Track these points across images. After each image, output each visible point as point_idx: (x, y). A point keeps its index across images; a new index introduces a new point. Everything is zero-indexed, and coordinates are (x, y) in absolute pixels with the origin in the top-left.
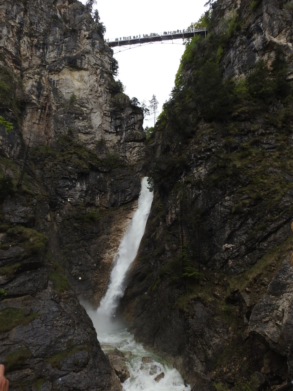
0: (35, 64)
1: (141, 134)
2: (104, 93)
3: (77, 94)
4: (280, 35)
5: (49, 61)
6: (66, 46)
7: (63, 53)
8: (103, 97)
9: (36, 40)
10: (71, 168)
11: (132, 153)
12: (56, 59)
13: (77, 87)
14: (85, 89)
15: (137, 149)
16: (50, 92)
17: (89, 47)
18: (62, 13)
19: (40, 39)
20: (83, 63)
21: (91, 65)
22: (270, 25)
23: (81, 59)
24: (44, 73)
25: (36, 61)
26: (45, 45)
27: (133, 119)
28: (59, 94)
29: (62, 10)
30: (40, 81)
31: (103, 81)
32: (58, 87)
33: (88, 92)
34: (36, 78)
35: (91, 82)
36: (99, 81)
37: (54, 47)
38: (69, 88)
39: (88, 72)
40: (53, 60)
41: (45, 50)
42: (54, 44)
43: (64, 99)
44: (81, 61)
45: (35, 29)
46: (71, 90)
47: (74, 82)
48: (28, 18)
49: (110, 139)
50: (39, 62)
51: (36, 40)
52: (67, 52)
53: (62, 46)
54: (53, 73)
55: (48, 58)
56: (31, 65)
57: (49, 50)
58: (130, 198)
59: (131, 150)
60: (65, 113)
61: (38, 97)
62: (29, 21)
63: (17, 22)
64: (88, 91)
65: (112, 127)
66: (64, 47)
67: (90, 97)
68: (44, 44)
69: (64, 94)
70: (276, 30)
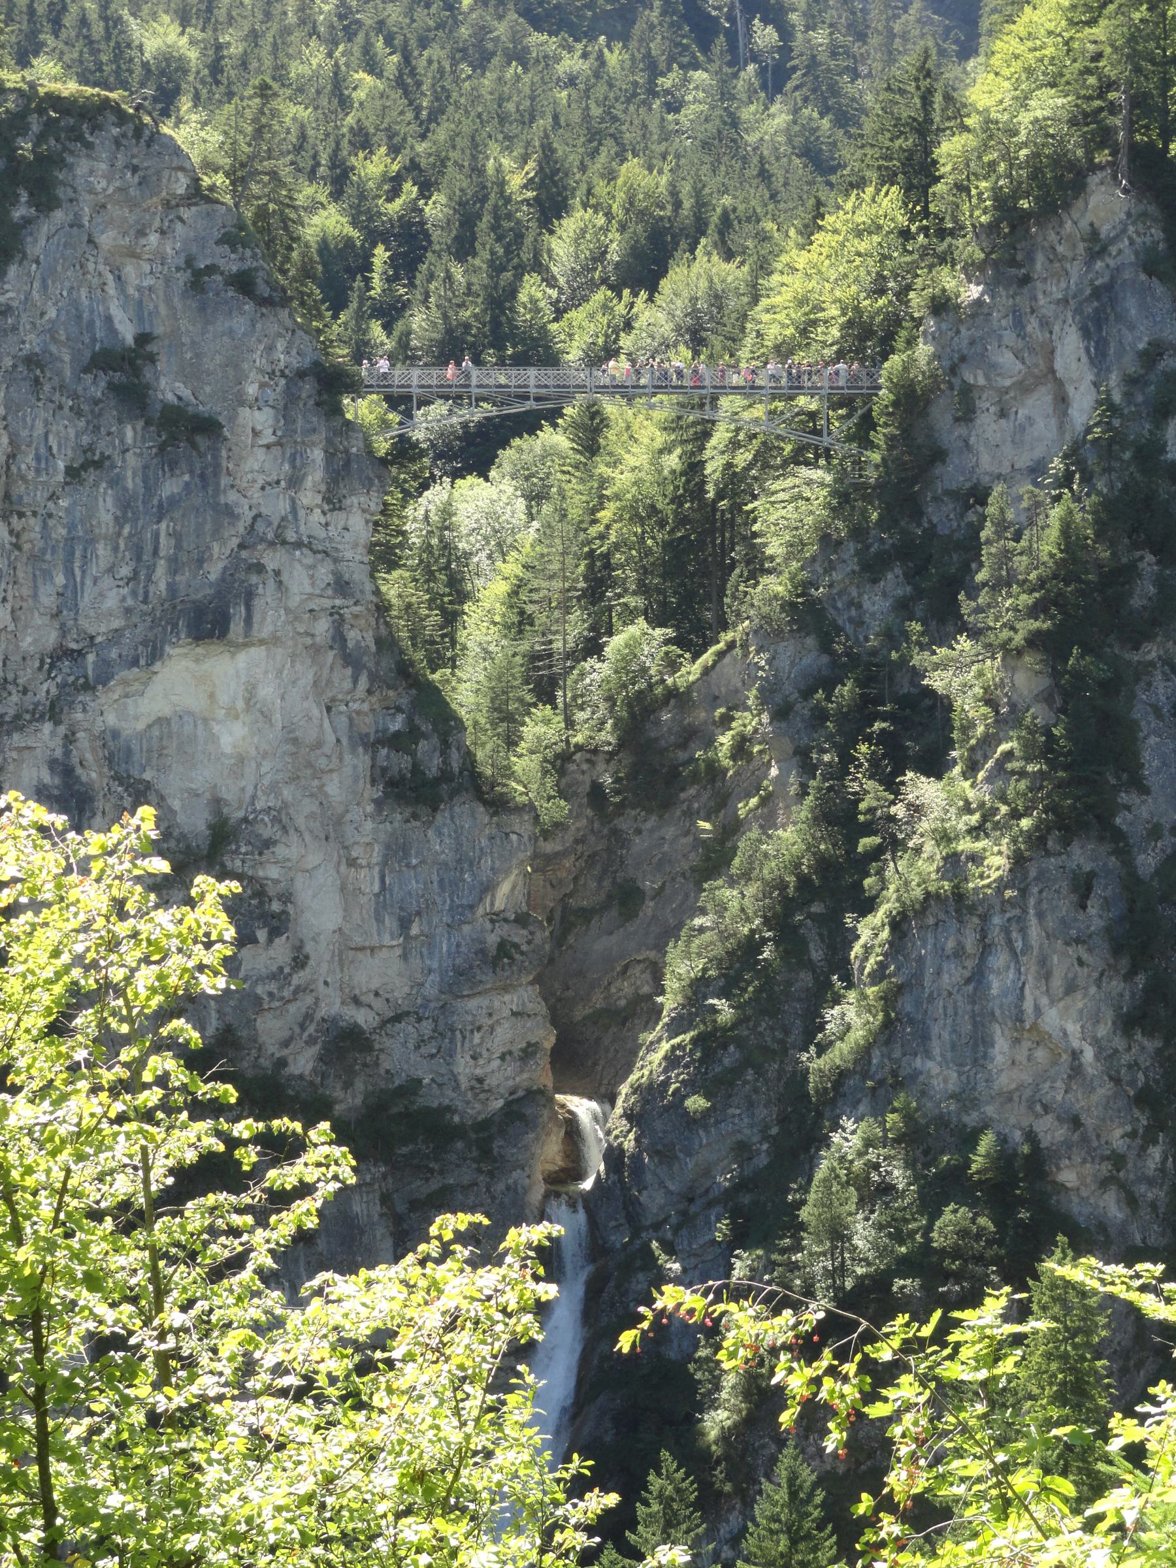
1: (524, 948)
2: (353, 750)
4: (1068, 999)
5: (101, 629)
6: (176, 536)
11: (485, 1054)
13: (228, 750)
14: (265, 755)
18: (131, 291)
20: (257, 618)
22: (1043, 962)
23: (249, 596)
24: (84, 710)
29: (129, 271)
30: (67, 753)
31: (347, 685)
32: (148, 776)
34: (52, 744)
37: (116, 549)
40: (117, 623)
41: (78, 572)
43: (183, 836)
45: (31, 475)
47: (216, 728)
49: (375, 985)
50: (51, 638)
51: (35, 523)
52: (175, 566)
54: (119, 691)
68: (70, 540)
70: (1057, 982)
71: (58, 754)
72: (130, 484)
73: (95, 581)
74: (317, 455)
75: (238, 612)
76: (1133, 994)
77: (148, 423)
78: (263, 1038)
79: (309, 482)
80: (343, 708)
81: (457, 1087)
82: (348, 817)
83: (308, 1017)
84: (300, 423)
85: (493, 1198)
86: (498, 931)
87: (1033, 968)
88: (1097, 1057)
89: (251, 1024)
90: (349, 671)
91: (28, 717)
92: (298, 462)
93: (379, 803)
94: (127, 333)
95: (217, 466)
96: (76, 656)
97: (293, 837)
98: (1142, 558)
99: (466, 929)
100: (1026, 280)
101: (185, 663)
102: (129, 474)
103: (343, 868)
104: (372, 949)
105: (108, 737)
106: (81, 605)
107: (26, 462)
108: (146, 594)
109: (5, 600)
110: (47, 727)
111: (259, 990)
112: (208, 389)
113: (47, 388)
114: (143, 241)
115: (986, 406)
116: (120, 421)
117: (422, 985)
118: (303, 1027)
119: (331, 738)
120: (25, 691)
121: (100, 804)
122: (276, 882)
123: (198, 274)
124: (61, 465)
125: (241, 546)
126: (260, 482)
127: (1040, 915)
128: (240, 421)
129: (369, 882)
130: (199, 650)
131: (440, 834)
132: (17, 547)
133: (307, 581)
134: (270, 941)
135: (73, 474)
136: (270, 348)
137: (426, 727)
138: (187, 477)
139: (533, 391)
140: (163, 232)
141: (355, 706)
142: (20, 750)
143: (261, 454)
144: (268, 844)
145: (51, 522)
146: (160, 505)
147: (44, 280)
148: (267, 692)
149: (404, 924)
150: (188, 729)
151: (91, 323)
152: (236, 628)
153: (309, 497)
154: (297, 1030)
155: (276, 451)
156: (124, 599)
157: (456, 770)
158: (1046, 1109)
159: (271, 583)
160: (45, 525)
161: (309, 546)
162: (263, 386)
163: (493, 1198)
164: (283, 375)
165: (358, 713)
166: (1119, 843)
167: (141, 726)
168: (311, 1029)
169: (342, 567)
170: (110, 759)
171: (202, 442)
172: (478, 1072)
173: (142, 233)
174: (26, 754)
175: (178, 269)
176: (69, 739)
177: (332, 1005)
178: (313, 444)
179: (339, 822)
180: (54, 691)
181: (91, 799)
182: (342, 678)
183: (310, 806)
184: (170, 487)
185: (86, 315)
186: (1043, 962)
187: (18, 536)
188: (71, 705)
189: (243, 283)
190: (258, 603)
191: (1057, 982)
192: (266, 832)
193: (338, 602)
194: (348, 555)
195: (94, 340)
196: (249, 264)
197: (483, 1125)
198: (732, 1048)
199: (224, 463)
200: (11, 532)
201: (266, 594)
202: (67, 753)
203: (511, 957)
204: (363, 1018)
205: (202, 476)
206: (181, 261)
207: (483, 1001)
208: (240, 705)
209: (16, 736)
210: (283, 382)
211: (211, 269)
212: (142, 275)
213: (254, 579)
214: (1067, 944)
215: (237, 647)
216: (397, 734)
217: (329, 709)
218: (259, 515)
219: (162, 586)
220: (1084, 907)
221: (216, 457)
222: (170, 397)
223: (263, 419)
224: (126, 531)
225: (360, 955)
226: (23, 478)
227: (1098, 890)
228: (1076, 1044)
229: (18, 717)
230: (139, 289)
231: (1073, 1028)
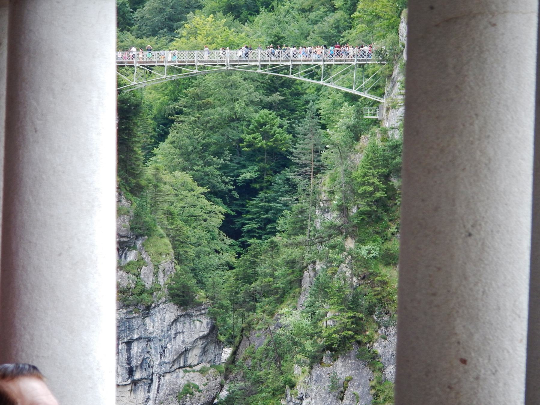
1: (202, 388)
27: (180, 338)
99: (168, 377)
131: (153, 321)
137: (147, 259)
149: (131, 372)
157: (162, 284)
203: (191, 394)
220: (342, 399)
227: (351, 390)
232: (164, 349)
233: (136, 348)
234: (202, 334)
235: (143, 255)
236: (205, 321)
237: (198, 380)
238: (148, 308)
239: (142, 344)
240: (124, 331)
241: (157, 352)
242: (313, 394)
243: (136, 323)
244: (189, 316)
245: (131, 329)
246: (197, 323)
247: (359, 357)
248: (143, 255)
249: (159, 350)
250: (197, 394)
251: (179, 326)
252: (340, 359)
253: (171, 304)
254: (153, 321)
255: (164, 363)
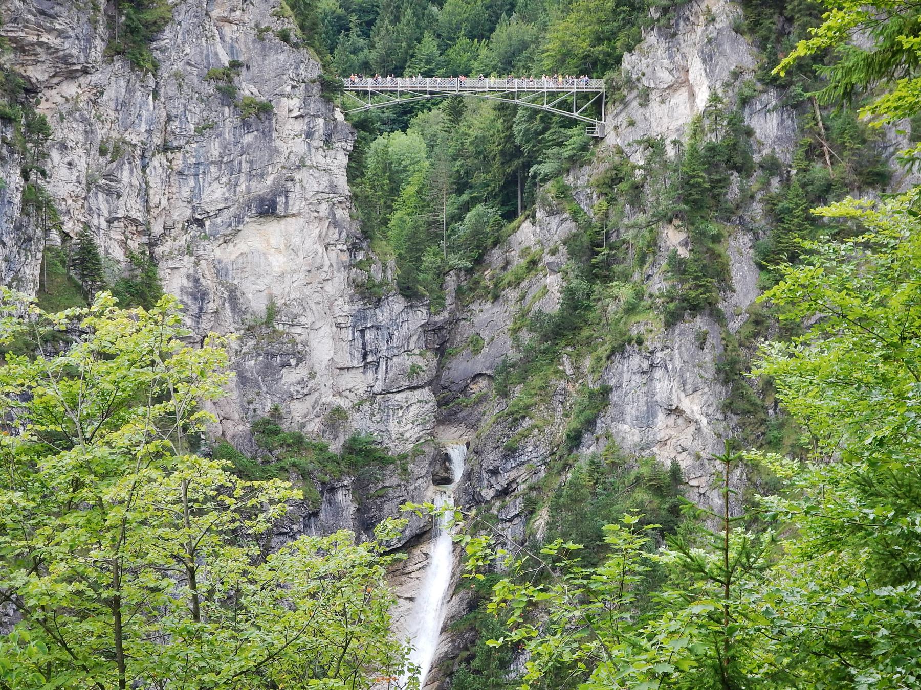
0: (178, 219)
1: (424, 368)
2: (339, 271)
3: (277, 290)
4: (694, 395)
5: (212, 209)
7: (242, 179)
8: (336, 279)
9: (179, 155)
10: (291, 508)
12: (229, 204)
13: (276, 269)
14: (295, 272)
15: (414, 410)
16: (224, 304)
17: (299, 146)
18: (227, 39)
19: (187, 152)
20: (291, 202)
21: (306, 200)
22: (681, 376)
23: (286, 193)
25: (182, 213)
26: (199, 168)
27: (405, 325)
28: (242, 300)
30: (196, 271)
31: (336, 236)
32: (236, 282)
33: (301, 277)
34: (188, 266)
35: (306, 246)
36: (326, 234)
37: (220, 169)
38: (259, 276)
39: (301, 221)
40: (221, 206)
41: (201, 180)
42: (221, 162)
43: (253, 314)
44: (286, 197)
45: (177, 131)
46: (265, 281)
47: (270, 258)
48: (162, 106)
50: (188, 213)
52: (250, 176)
53: (240, 163)
55: (207, 200)
56: (170, 223)
57: (209, 178)
58: (399, 540)
59: (400, 414)
60: (259, 355)
61: (198, 318)
62: (165, 114)
63: (143, 130)
64: (302, 275)
65: (356, 354)
66: (244, 164)
67: (307, 290)
69: (250, 296)
71: (191, 271)
72: (227, 136)
73: (210, 183)
74: (320, 122)
75: (281, 200)
76: (727, 392)
77: (236, 106)
78: (294, 414)
79: (316, 135)
80: (333, 248)
81: (391, 438)
82: (336, 303)
83: (316, 402)
84: (312, 105)
85: (408, 493)
86: (411, 360)
87: (677, 379)
88: (709, 423)
89: (288, 407)
90: (337, 230)
91: (176, 252)
92: (311, 126)
93: (351, 296)
94: (225, 60)
95: (271, 126)
96: (200, 223)
97: (309, 313)
98: (732, 174)
99: (395, 359)
100: (674, 35)
101: (254, 225)
102: (227, 130)
103: (334, 328)
104: (348, 368)
105: (216, 262)
106: (203, 197)
107: (174, 125)
108: (235, 192)
109: (164, 194)
110: (186, 257)
111: (292, 389)
112: (266, 88)
113: (185, 88)
114: (233, 14)
115: (654, 96)
116: (223, 105)
117: (372, 387)
118: (313, 408)
119: (327, 263)
120: (175, 240)
121: (211, 296)
122: (300, 335)
123: (261, 31)
124: (192, 127)
125: (283, 167)
126: (292, 135)
127: (680, 353)
128: (282, 104)
129: (347, 334)
130: (262, 219)
131: (382, 311)
132: (170, 167)
133: (316, 185)
134: (297, 365)
135: (200, 131)
136: (297, 68)
137: (376, 258)
138: (256, 133)
139: (429, 89)
140: (243, 10)
141: (340, 247)
142: (172, 269)
143: (292, 120)
144: (296, 316)
145: (187, 155)
146: (242, 147)
147: (183, 34)
148: (296, 240)
149: (365, 356)
150: (256, 259)
151: (207, 56)
152: (280, 209)
153: (317, 142)
154: (311, 409)
155: (300, 120)
156: (224, 194)
157: (390, 279)
158: (684, 450)
159: (298, 185)
160: (184, 157)
161: (317, 167)
162: (293, 87)
163: (408, 493)
164: (303, 82)
165: (341, 251)
166: (718, 317)
167: (233, 257)
168: (318, 409)
169: (333, 178)
170: (218, 274)
171: (262, 116)
172: (401, 430)
173: (232, 10)
174: (175, 271)
175: (251, 28)
176: (197, 263)
177: (328, 398)
178: (319, 116)
179: (331, 306)
180: (189, 239)
181: (208, 294)
182: (334, 234)
183: (317, 297)
184: (248, 139)
185: (205, 52)
186: (681, 376)
187: (171, 162)
188: (197, 246)
189: (284, 37)
190: (290, 195)
191: (688, 386)
192: (296, 310)
193: (331, 195)
194: (336, 171)
195: (209, 64)
196: (287, 26)
197: (404, 457)
198: (527, 419)
199: (274, 125)
200: (168, 160)
201: (295, 191)
202: (196, 271)
203: (417, 373)
204: (344, 403)
205: (263, 132)
206: (253, 24)
207: (404, 395)
208: (282, 247)
209: (170, 262)
210: (303, 85)
211: (268, 29)
212: (233, 32)
213: (289, 184)
214: (694, 367)
215: (279, 217)
216: (361, 262)
217: (327, 249)
218: (291, 152)
219: (243, 187)
220: (703, 349)
221: (269, 123)
222: (247, 93)
223: (295, 103)
224: (225, 160)
225: (342, 372)
226: (173, 133)
227: (709, 341)
228: (698, 417)
229: (171, 253)
230: (232, 39)
231: (696, 408)
232: (391, 335)
233: (369, 335)
234: (423, 322)
235: (371, 255)
236: (425, 311)
237: (421, 362)
238: (379, 300)
239: (374, 332)
240: (360, 320)
241: (383, 339)
242: (677, 346)
243: (370, 313)
244: (411, 307)
245: (365, 319)
246: (419, 313)
247: (711, 315)
248: (371, 255)
249: (386, 336)
250: (421, 373)
251: (404, 316)
252: (698, 316)
253: (400, 296)
254: (382, 311)
255: (393, 347)
